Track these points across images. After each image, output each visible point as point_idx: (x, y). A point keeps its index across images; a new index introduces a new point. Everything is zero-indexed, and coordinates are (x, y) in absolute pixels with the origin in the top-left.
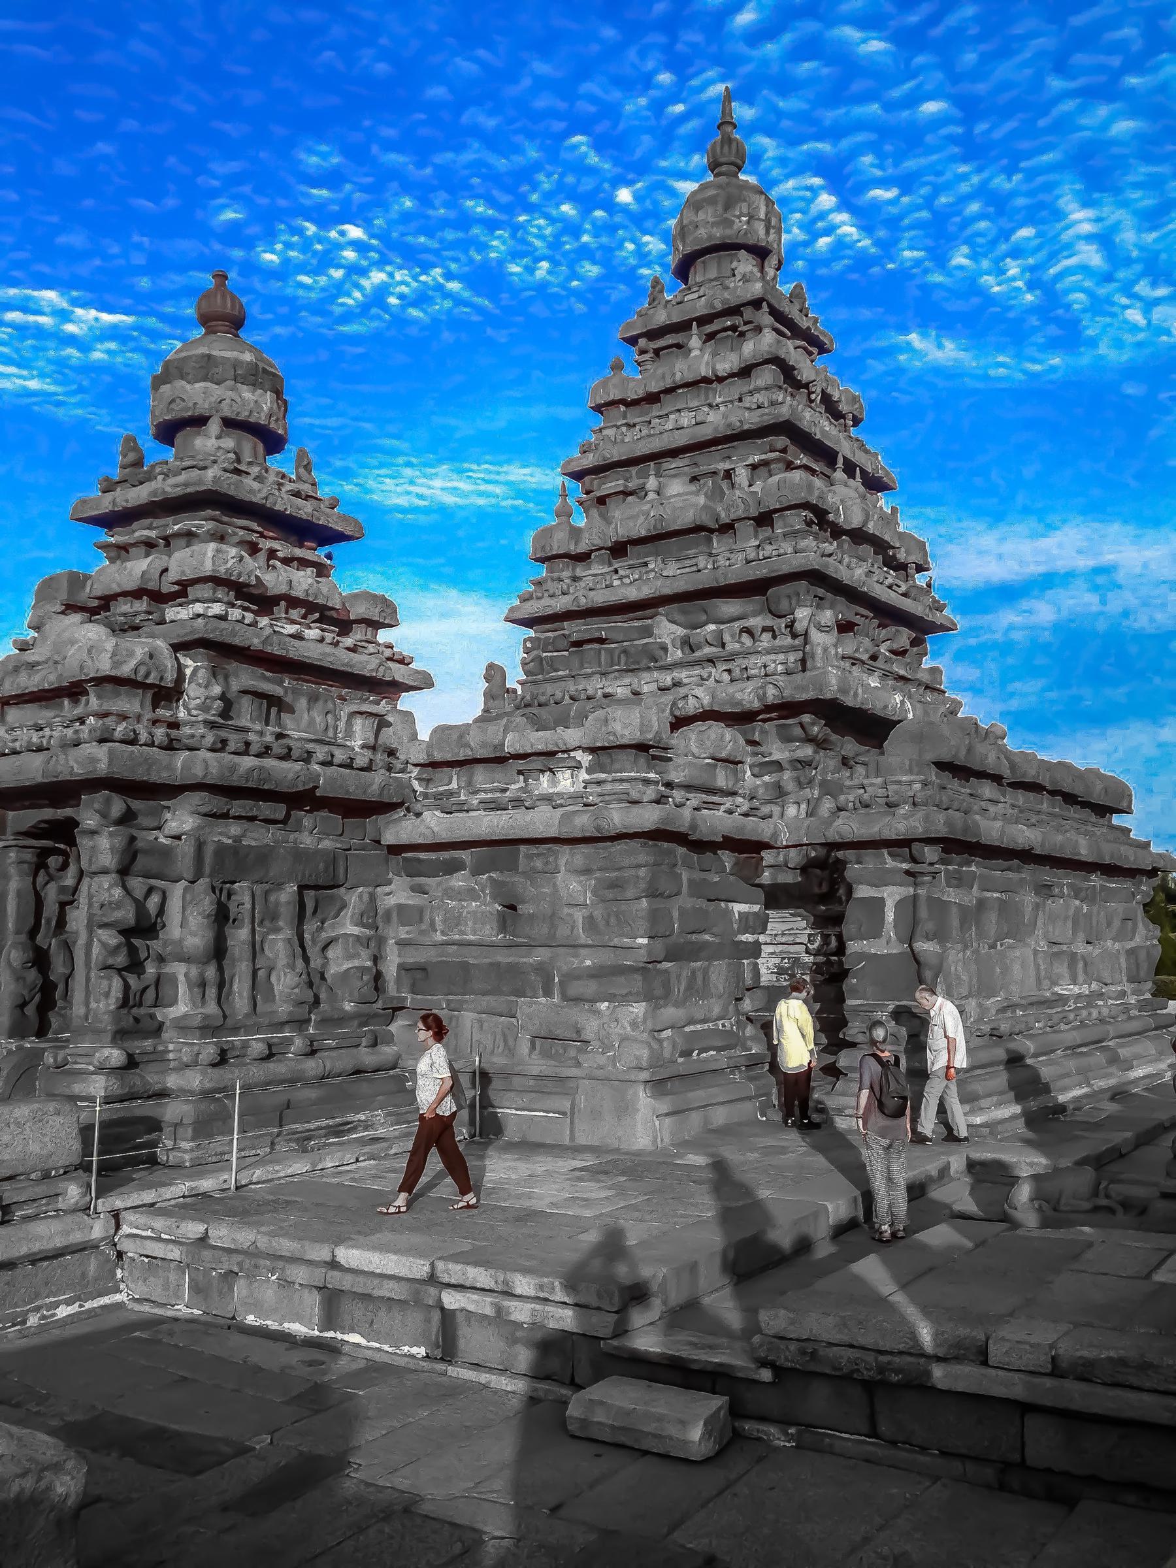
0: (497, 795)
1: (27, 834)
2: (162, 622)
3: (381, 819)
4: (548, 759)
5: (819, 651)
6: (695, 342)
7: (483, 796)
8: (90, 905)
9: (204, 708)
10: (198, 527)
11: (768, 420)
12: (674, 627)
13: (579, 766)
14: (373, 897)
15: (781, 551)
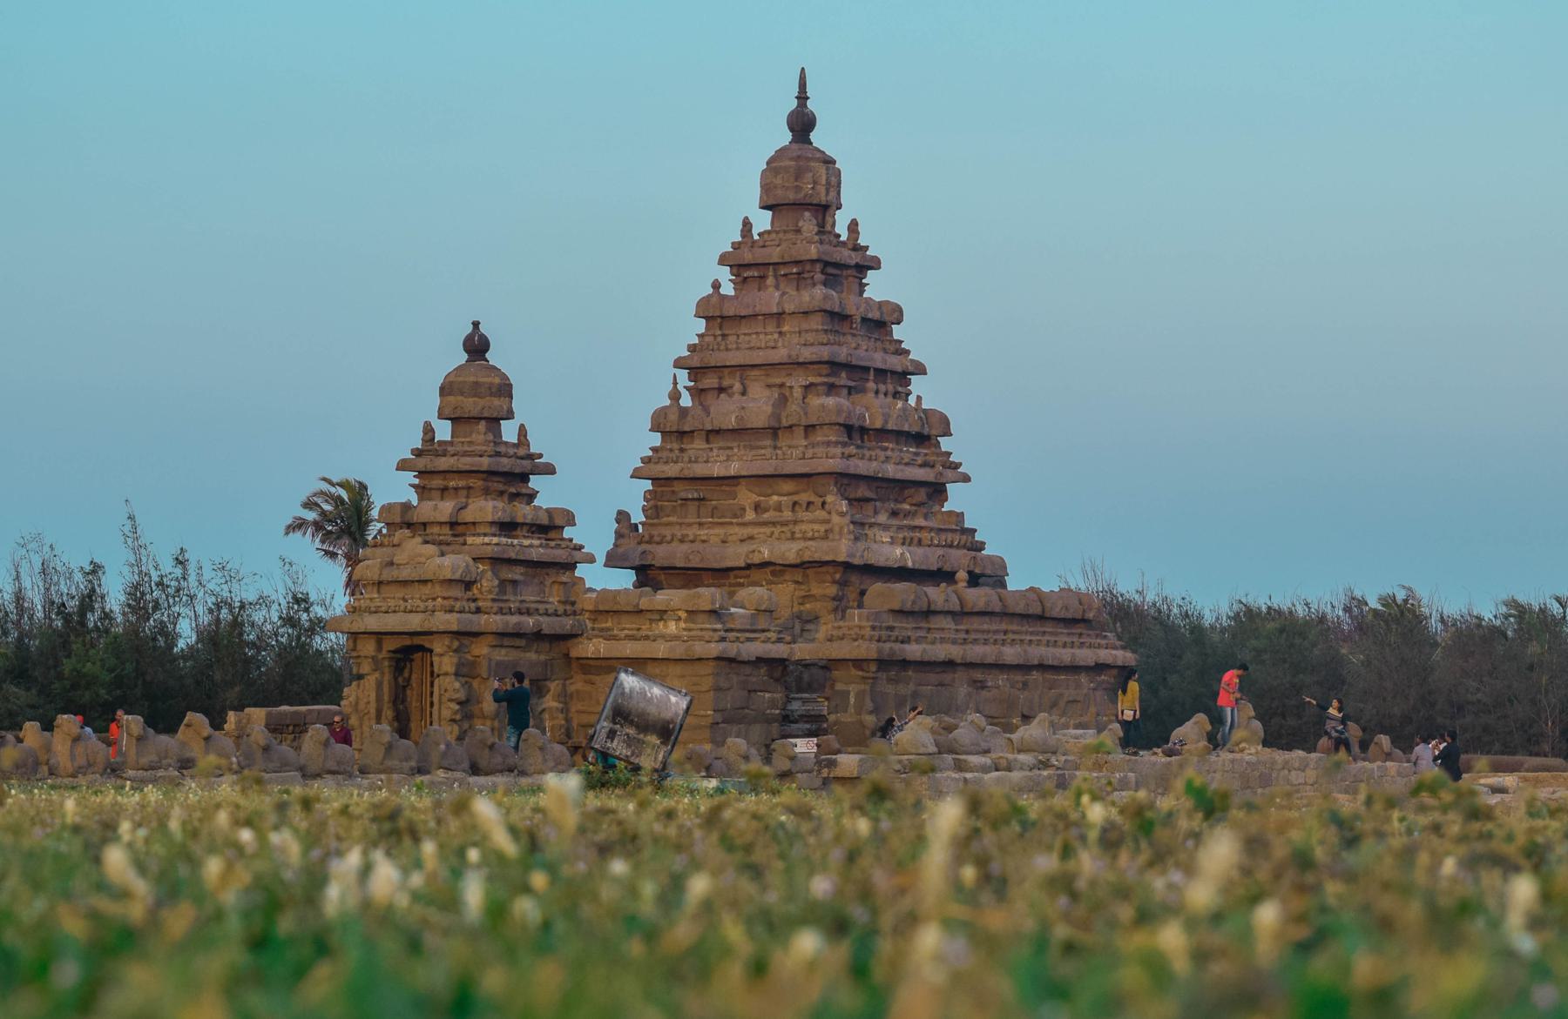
0: (635, 632)
1: (394, 652)
2: (465, 544)
3: (570, 643)
4: (662, 614)
5: (837, 529)
6: (770, 281)
7: (626, 632)
8: (440, 690)
9: (490, 592)
10: (476, 483)
11: (814, 358)
12: (750, 494)
13: (680, 619)
14: (564, 685)
15: (819, 455)
